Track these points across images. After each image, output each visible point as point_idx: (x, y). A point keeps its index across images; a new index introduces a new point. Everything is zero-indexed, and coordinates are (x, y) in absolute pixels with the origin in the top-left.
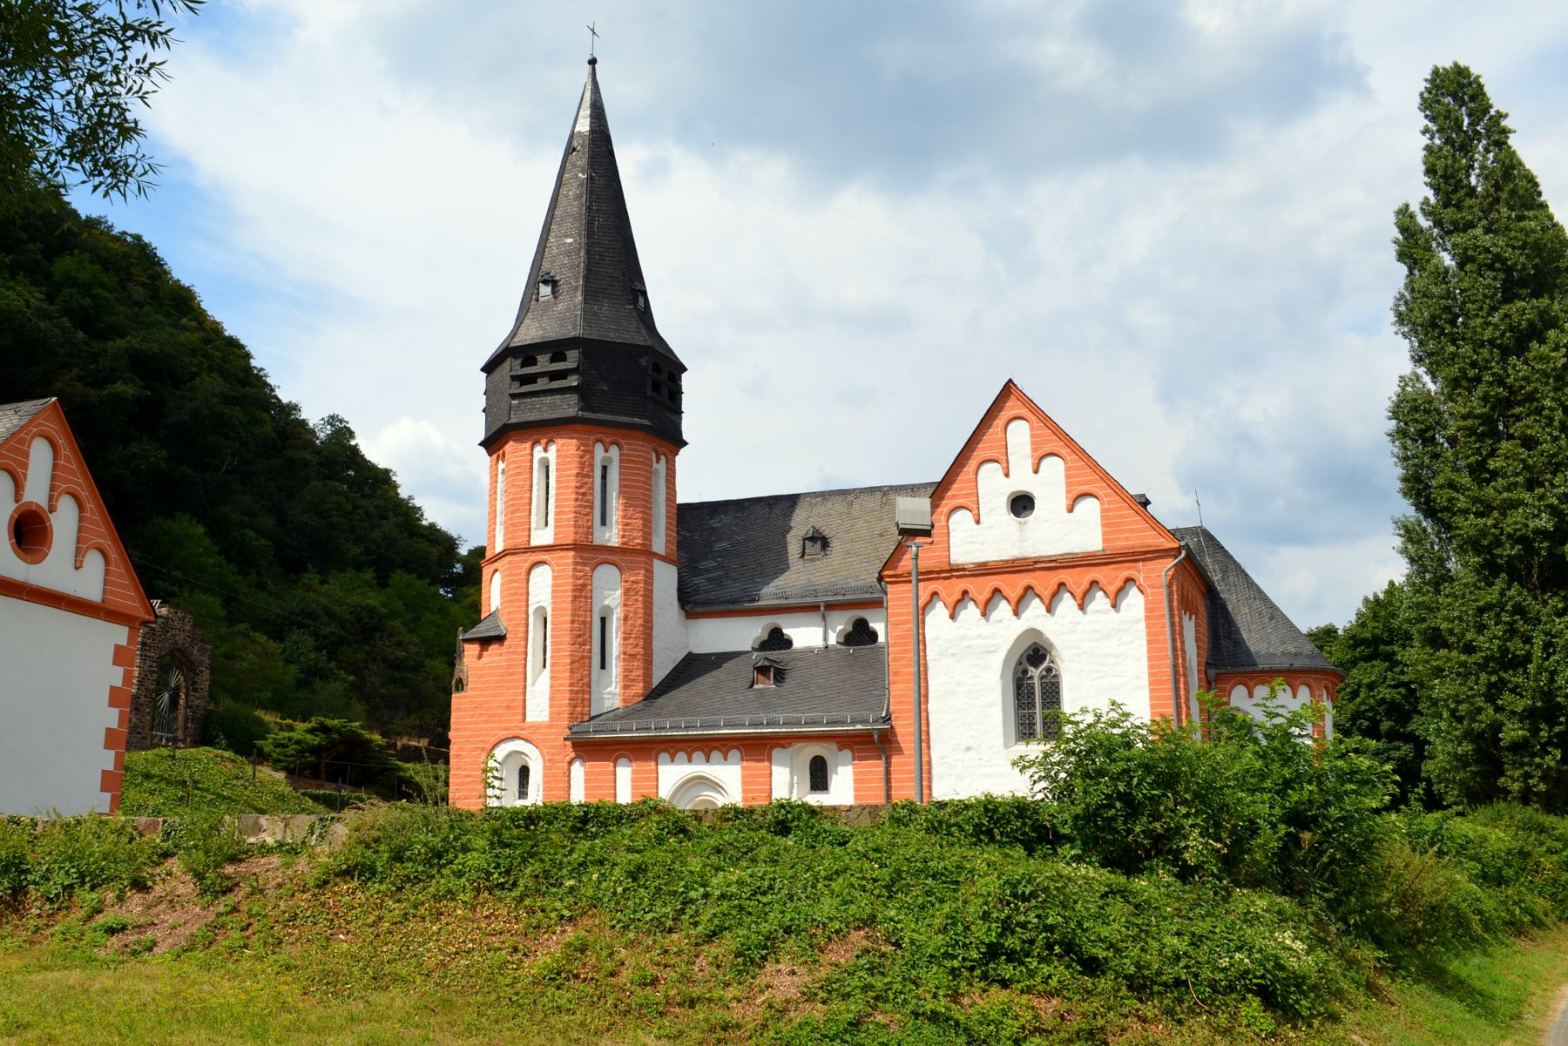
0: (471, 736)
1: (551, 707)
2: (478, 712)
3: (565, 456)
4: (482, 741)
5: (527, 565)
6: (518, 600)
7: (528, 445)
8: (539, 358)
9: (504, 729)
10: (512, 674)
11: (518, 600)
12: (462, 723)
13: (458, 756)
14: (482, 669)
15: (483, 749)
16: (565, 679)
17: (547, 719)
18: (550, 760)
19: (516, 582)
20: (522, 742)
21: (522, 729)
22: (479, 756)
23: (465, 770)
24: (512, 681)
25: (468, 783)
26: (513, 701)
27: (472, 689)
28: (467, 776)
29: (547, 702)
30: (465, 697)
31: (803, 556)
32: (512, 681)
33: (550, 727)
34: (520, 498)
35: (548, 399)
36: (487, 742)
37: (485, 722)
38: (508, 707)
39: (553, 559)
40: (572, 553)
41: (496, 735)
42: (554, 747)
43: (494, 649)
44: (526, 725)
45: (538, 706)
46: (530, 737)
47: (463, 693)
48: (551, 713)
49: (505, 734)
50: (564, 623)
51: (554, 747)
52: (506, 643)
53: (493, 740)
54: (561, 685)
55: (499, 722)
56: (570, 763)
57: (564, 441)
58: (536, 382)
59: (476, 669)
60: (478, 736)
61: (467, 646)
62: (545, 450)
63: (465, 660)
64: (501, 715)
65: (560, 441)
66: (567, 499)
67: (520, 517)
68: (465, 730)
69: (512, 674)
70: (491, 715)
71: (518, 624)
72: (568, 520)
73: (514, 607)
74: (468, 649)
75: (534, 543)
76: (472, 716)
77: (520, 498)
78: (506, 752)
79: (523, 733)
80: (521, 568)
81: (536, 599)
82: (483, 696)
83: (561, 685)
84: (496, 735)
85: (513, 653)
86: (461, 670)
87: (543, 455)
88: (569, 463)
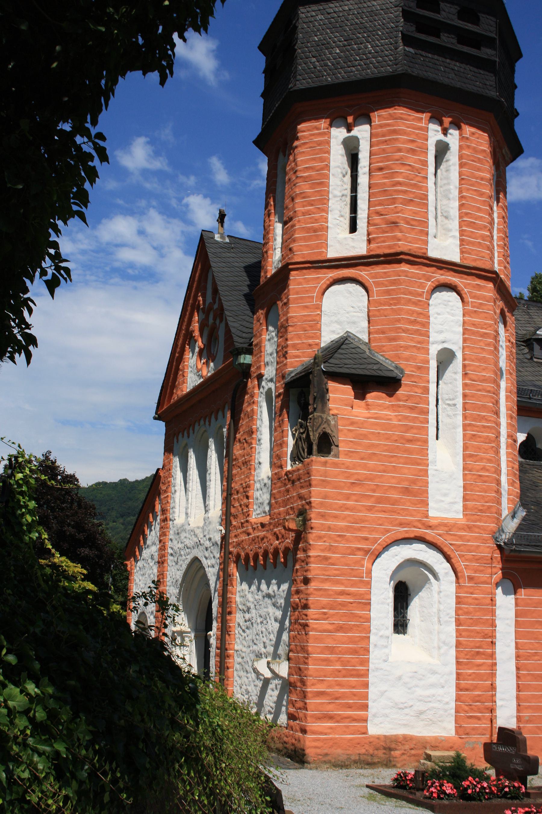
0: (348, 529)
1: (465, 499)
2: (357, 491)
3: (475, 150)
4: (366, 539)
5: (429, 285)
6: (417, 332)
7: (425, 116)
8: (442, 5)
9: (401, 524)
10: (410, 441)
11: (417, 332)
12: (331, 508)
13: (326, 558)
14: (361, 424)
15: (366, 552)
16: (489, 461)
17: (461, 516)
18: (471, 578)
19: (416, 304)
20: (422, 546)
21: (430, 527)
22: (359, 563)
23: (338, 582)
24: (408, 451)
25: (343, 605)
26: (414, 482)
27: (348, 454)
28: (342, 593)
29: (460, 493)
30: (336, 465)
31: (531, 358)
32: (408, 451)
33: (469, 528)
34: (415, 186)
35: (457, 66)
36: (376, 540)
37: (370, 509)
38: (406, 491)
39: (466, 285)
40: (491, 285)
41: (388, 531)
42: (477, 560)
43: (374, 397)
44: (433, 522)
45: (446, 495)
46: (440, 541)
47: (330, 459)
48: (465, 508)
49: (402, 533)
50: (485, 380)
51: (477, 560)
52: (400, 392)
53: (383, 539)
54: (484, 469)
55: (394, 512)
56: (497, 585)
57: (473, 130)
58: (438, 37)
59: (352, 423)
60: (359, 529)
61: (332, 385)
62: (445, 132)
63: (331, 405)
64: (395, 502)
65: (468, 130)
66: (479, 210)
67: (416, 213)
68: (336, 517)
69: (410, 441)
70: (379, 500)
71: (419, 368)
72: (483, 237)
73: (412, 340)
74: (336, 391)
75: (432, 253)
76: (348, 497)
77: (415, 186)
78: (399, 560)
79: (430, 534)
80: (422, 286)
81: (441, 337)
82: (365, 467)
83: (484, 469)
84: (388, 531)
85: (412, 409)
86: (328, 422)
87: (441, 137)
88: (480, 161)
